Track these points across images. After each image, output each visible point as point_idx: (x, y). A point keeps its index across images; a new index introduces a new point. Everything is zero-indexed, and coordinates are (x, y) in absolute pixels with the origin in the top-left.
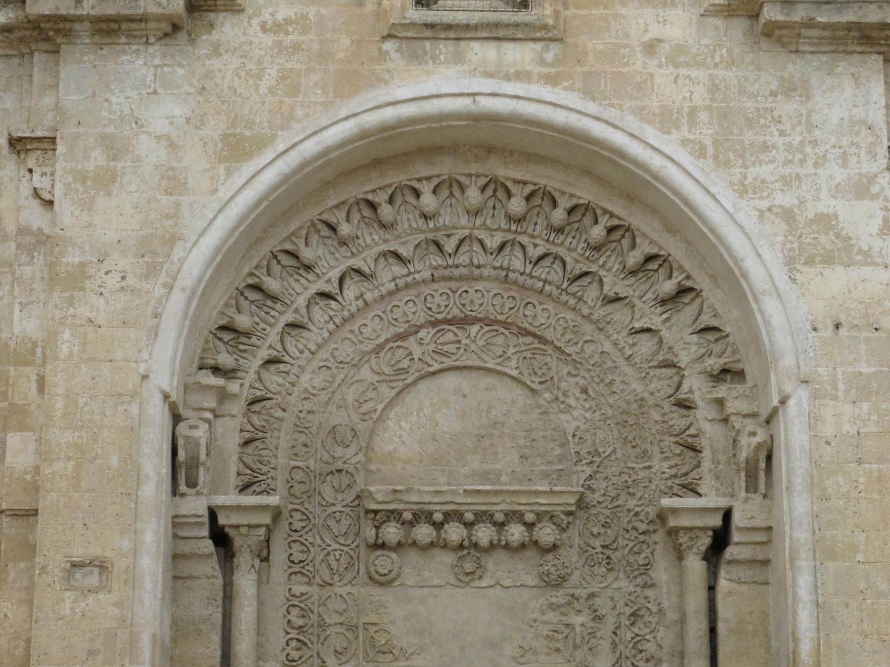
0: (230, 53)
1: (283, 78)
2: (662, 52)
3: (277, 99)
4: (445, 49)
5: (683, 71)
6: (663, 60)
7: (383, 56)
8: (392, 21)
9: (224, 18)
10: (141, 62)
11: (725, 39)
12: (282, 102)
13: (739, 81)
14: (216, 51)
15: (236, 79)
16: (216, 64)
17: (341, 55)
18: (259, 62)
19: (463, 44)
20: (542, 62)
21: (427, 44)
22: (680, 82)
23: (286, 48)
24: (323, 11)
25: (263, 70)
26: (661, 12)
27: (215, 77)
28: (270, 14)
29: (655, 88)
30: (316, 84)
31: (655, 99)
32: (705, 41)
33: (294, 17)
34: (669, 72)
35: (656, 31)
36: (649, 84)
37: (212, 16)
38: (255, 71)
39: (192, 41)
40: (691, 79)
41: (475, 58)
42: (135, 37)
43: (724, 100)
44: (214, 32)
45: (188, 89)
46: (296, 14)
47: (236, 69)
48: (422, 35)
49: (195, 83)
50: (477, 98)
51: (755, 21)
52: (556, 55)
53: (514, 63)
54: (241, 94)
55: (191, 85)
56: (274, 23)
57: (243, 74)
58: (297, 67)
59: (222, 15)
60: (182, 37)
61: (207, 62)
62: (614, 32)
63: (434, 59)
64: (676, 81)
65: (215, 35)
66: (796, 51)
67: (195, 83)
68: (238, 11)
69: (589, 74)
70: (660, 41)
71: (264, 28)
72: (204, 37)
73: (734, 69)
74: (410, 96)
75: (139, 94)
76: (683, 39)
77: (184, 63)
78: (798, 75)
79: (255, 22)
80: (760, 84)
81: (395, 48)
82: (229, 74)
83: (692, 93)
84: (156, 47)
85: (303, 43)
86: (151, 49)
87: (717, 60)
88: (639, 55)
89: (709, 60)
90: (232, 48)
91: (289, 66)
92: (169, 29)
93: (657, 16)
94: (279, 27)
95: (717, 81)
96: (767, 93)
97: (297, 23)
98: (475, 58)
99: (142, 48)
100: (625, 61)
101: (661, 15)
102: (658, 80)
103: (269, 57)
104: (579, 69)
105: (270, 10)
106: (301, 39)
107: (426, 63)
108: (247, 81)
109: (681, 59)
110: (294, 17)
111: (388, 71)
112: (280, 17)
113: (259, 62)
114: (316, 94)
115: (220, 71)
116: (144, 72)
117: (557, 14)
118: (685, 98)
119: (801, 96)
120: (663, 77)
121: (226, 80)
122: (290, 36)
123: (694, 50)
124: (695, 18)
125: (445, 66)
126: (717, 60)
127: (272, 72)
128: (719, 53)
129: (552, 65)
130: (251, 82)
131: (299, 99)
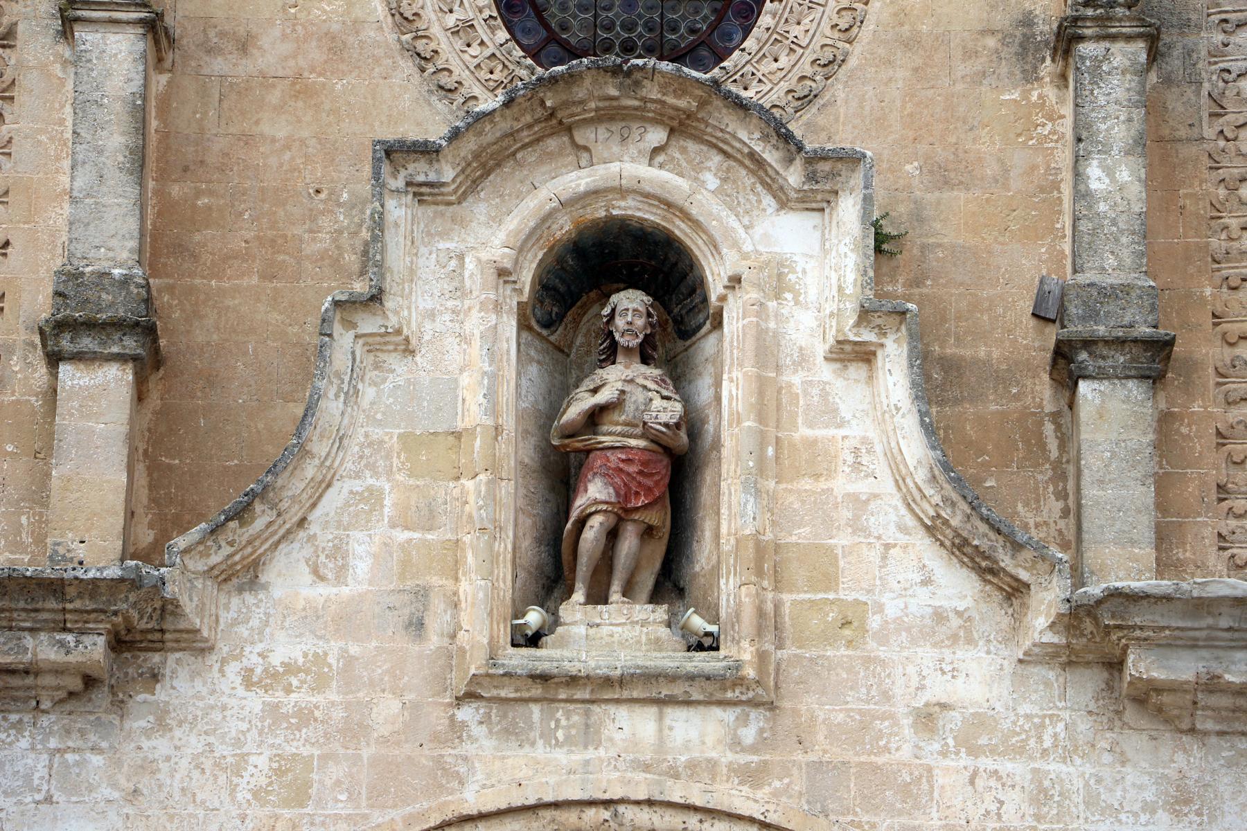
0: (186, 727)
1: (280, 772)
2: (948, 727)
3: (268, 810)
4: (567, 719)
5: (986, 763)
6: (951, 742)
7: (457, 730)
8: (473, 671)
9: (178, 661)
10: (24, 743)
11: (1060, 705)
12: (277, 817)
13: (1087, 784)
14: (162, 725)
15: (196, 774)
16: (160, 746)
17: (385, 730)
18: (238, 743)
19: (595, 708)
20: (736, 744)
21: (536, 709)
22: (980, 783)
23: (286, 717)
24: (354, 650)
25: (244, 757)
26: (947, 654)
27: (159, 770)
28: (259, 655)
29: (936, 795)
30: (338, 783)
31: (935, 815)
32: (1025, 708)
33: (301, 661)
34: (962, 763)
35: (938, 689)
36: (925, 786)
37: (156, 658)
38: (230, 759)
39: (119, 706)
40: (999, 778)
41: (618, 736)
42: (15, 699)
43: (1059, 818)
44: (158, 686)
45: (106, 792)
46: (305, 655)
47: (195, 757)
48: (526, 695)
49: (123, 781)
50: (621, 809)
51: (1116, 674)
52: (761, 731)
53: (687, 746)
54: (203, 802)
55: (114, 785)
56: (266, 670)
57: (208, 764)
58: (305, 751)
59: (172, 657)
60: (101, 697)
61: (146, 744)
62: (864, 690)
63: (548, 737)
64: (972, 782)
65: (161, 694)
66: (1192, 731)
67: (123, 781)
68: (202, 650)
69: (817, 766)
70: (944, 706)
71: (248, 681)
72: (140, 697)
73: (1078, 761)
74: (503, 806)
75: (19, 803)
76: (986, 705)
77: (104, 745)
78: (1195, 775)
79: (233, 668)
80: (1124, 790)
81: (478, 718)
82: (184, 763)
83: (1002, 803)
84: (53, 717)
85: (317, 708)
86: (45, 721)
87: (1047, 743)
88: (907, 732)
89: (1032, 742)
90: (190, 717)
91: (290, 749)
92: (76, 684)
93: (941, 660)
94: (273, 678)
95: (1047, 783)
96: (1137, 807)
97: (307, 672)
98: (618, 736)
99: (27, 718)
100: (882, 743)
101: (948, 660)
102: (940, 780)
103: (254, 731)
104: (799, 757)
105: (259, 647)
106: (314, 700)
107: (533, 744)
108: (216, 777)
109: (983, 741)
110: (301, 661)
111: (465, 759)
112: (276, 660)
113: (238, 743)
114: (337, 801)
115: (168, 759)
116: (29, 761)
117: (762, 657)
118: (988, 812)
119: (1199, 813)
120: (950, 773)
121: (178, 776)
122: (293, 695)
123: (1006, 725)
124: (1009, 667)
125: (565, 749)
126: (1047, 743)
127: (261, 761)
128: (1050, 730)
129: (753, 749)
130: (222, 779)
131: (308, 810)
